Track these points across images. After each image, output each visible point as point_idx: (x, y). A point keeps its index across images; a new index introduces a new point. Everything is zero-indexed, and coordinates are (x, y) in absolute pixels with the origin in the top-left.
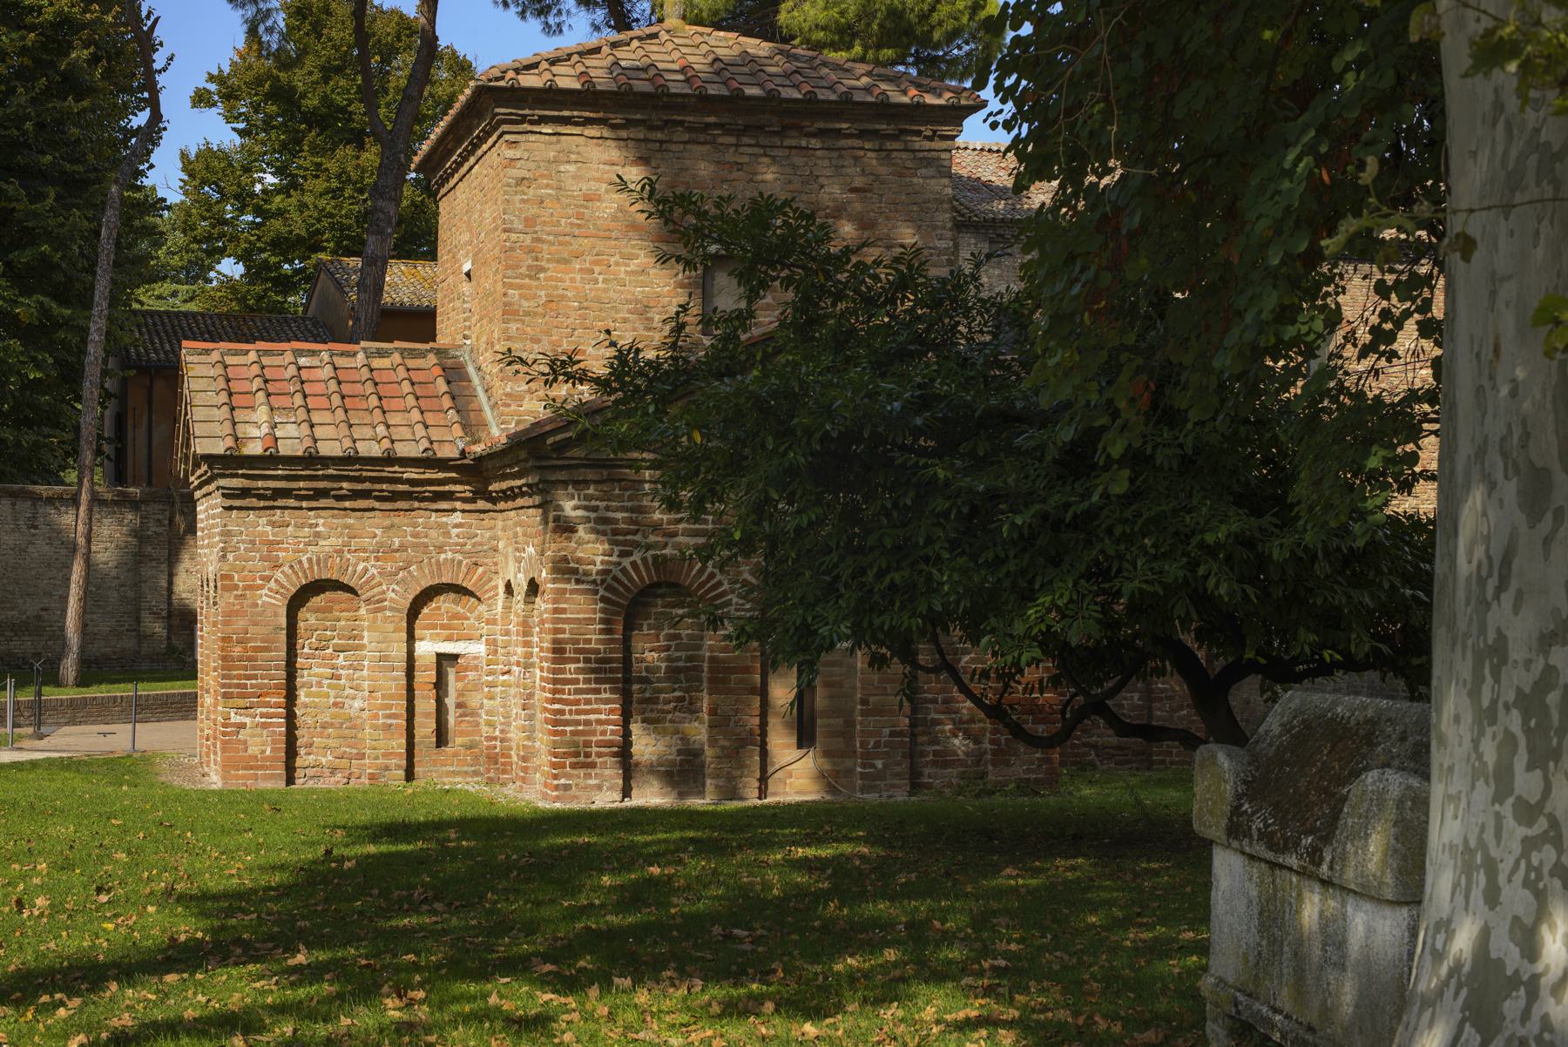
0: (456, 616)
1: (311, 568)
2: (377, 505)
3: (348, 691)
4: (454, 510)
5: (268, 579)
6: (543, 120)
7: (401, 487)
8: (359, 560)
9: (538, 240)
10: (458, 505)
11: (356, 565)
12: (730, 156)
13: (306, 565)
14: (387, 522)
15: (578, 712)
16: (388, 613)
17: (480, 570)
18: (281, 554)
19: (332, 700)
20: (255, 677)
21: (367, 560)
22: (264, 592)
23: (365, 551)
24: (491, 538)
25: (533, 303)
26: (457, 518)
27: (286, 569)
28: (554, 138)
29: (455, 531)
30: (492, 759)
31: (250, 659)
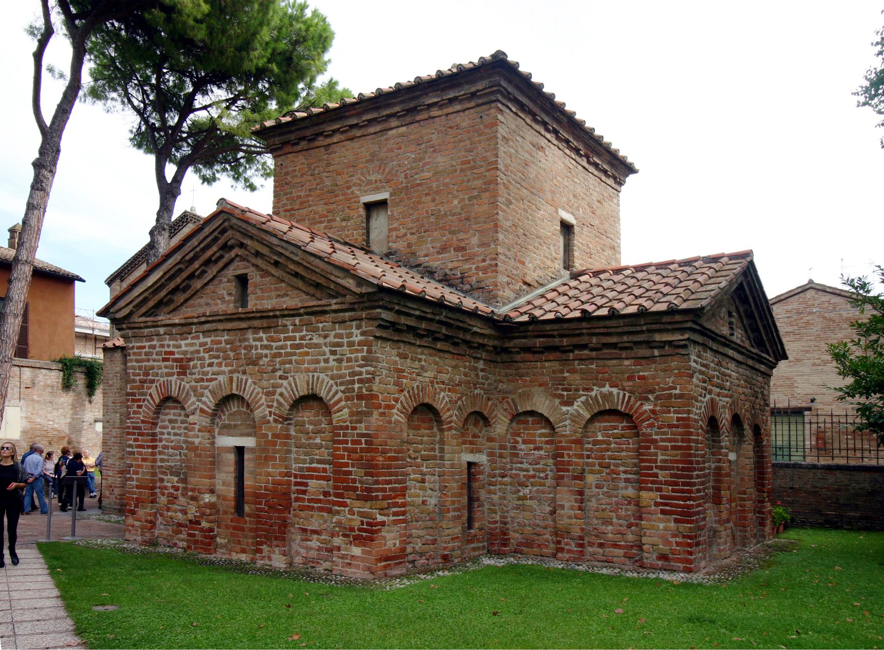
0: (474, 436)
1: (418, 394)
2: (451, 349)
3: (430, 492)
4: (479, 359)
5: (396, 400)
8: (441, 390)
10: (484, 355)
11: (439, 394)
13: (416, 391)
14: (454, 363)
16: (454, 432)
17: (490, 403)
18: (405, 381)
21: (444, 390)
22: (395, 411)
23: (443, 383)
24: (495, 381)
26: (481, 365)
27: (406, 392)
29: (481, 374)
30: (491, 536)
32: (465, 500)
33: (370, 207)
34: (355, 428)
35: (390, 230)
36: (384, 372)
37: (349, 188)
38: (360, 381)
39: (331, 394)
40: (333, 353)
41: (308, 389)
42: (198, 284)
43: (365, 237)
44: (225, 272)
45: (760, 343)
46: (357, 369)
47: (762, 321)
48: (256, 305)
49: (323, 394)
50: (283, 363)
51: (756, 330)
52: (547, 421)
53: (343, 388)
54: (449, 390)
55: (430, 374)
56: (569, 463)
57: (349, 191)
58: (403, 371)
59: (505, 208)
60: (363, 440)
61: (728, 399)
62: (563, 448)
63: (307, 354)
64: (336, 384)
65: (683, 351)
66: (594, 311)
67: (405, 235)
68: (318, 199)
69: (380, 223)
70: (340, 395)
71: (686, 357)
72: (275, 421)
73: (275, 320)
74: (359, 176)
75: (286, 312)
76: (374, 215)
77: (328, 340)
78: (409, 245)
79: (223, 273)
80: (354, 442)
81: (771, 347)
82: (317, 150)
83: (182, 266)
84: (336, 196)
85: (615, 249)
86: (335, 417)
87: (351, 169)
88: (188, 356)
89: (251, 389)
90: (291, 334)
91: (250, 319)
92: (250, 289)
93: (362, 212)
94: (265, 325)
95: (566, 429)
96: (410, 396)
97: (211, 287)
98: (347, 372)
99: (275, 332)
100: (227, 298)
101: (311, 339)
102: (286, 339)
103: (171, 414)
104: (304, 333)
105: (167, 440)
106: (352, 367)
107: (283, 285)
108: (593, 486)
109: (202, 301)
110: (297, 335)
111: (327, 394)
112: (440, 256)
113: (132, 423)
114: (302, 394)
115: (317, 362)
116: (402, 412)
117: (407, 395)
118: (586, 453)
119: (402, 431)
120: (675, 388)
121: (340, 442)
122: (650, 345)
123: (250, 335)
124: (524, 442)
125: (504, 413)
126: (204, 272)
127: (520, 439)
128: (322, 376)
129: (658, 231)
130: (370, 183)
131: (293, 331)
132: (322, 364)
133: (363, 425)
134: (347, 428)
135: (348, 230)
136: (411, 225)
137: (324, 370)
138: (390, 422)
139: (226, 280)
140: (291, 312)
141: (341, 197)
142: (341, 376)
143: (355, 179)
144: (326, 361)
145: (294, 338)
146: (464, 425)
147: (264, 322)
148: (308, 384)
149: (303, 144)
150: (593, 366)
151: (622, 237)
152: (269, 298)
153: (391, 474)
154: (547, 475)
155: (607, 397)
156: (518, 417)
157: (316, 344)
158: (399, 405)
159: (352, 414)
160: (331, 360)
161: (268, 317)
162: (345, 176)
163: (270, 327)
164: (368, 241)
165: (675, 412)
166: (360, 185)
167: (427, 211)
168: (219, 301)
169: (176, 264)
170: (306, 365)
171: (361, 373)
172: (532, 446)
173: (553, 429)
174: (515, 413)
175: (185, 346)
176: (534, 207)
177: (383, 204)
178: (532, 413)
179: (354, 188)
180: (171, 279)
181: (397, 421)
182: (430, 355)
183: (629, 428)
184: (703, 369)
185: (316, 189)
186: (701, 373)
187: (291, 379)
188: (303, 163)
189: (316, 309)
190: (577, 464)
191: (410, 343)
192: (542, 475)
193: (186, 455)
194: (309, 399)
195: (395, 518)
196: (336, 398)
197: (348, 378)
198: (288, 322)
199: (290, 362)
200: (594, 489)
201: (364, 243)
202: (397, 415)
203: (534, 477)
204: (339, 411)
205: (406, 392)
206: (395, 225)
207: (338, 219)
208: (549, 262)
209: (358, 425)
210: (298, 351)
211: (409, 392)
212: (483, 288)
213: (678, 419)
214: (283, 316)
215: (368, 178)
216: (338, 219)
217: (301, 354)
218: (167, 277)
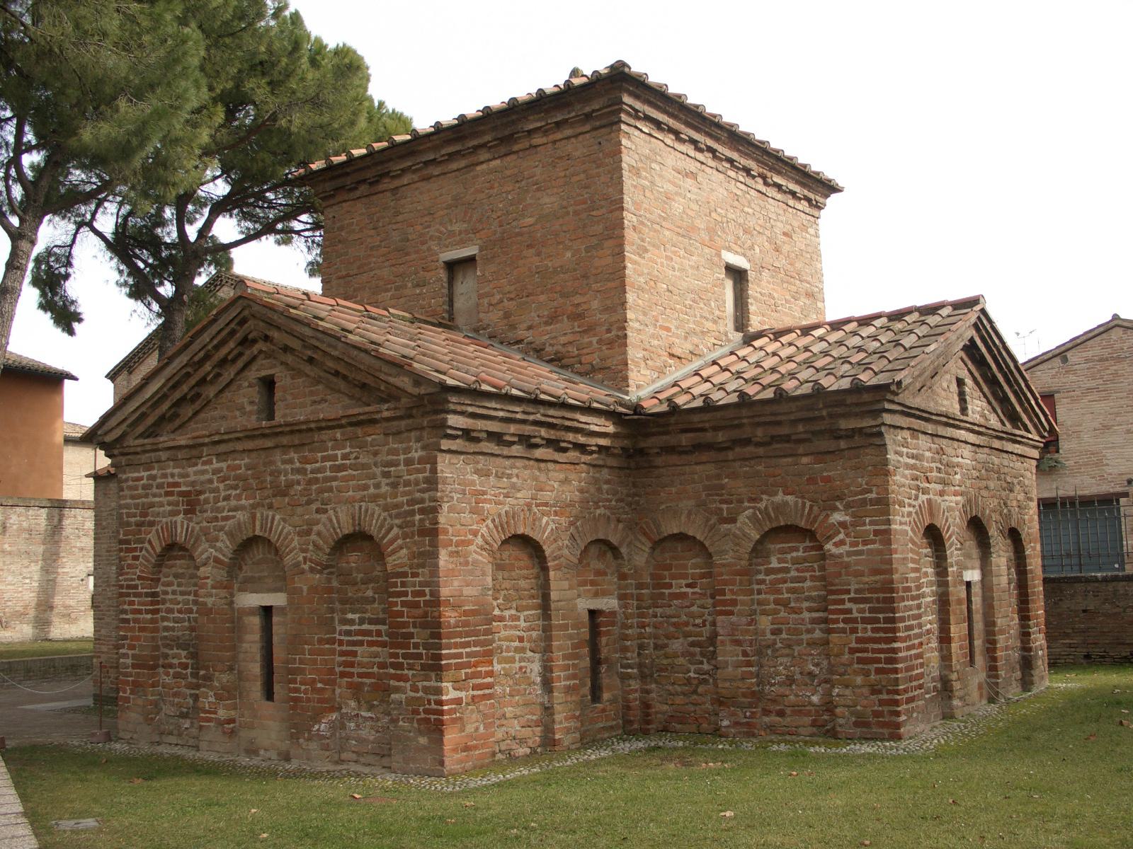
5: (475, 533)
6: (648, 118)
7: (582, 439)
9: (642, 223)
11: (540, 520)
12: (732, 186)
13: (504, 519)
14: (562, 476)
15: (909, 648)
19: (517, 665)
20: (467, 645)
21: (548, 514)
22: (473, 548)
23: (546, 504)
25: (642, 280)
27: (489, 522)
28: (648, 138)
29: (605, 487)
31: (466, 624)
32: (586, 662)
33: (453, 267)
34: (415, 575)
35: (481, 297)
36: (456, 496)
37: (423, 243)
38: (422, 511)
39: (383, 531)
40: (386, 475)
41: (354, 525)
42: (211, 391)
43: (446, 307)
44: (246, 373)
45: (1014, 418)
46: (418, 495)
47: (1011, 386)
48: (285, 416)
49: (373, 531)
50: (321, 491)
51: (1004, 400)
52: (702, 544)
53: (397, 521)
54: (556, 513)
55: (524, 495)
56: (734, 603)
57: (424, 247)
58: (484, 493)
59: (636, 258)
60: (427, 590)
61: (959, 498)
62: (726, 583)
63: (353, 478)
64: (390, 516)
65: (877, 441)
66: (758, 393)
67: (501, 301)
68: (381, 259)
69: (466, 287)
70: (395, 530)
71: (882, 449)
72: (312, 570)
73: (310, 434)
74: (438, 226)
75: (323, 424)
76: (460, 277)
77: (379, 458)
78: (507, 315)
79: (241, 376)
80: (416, 594)
81: (1031, 420)
82: (381, 195)
83: (189, 370)
84: (407, 254)
85: (814, 296)
86: (391, 561)
87: (426, 219)
88: (198, 488)
89: (281, 526)
90: (331, 452)
91: (277, 434)
92: (278, 394)
93: (443, 275)
94: (297, 442)
95: (728, 556)
96: (496, 527)
97: (227, 394)
98: (405, 499)
99: (310, 451)
100: (248, 408)
101: (356, 458)
102: (324, 459)
103: (180, 565)
104: (348, 450)
105: (172, 601)
106: (409, 493)
107: (320, 387)
108: (768, 631)
109: (216, 413)
110: (339, 453)
111: (379, 532)
112: (549, 328)
113: (126, 580)
114: (347, 532)
115: (366, 487)
116: (485, 549)
117: (491, 526)
118: (756, 587)
119: (484, 574)
120: (871, 492)
121: (400, 594)
122: (836, 435)
123: (278, 456)
124: (673, 577)
125: (644, 539)
126: (218, 375)
127: (666, 573)
128: (371, 505)
129: (864, 267)
130: (451, 234)
131: (333, 449)
132: (372, 490)
133: (426, 571)
134: (404, 575)
135: (424, 299)
136: (508, 288)
137: (374, 498)
138: (467, 563)
139: (246, 384)
140: (330, 424)
141: (414, 256)
142: (397, 506)
143: (432, 231)
144: (377, 486)
145: (334, 458)
146: (580, 561)
147: (296, 439)
148: (353, 518)
149: (363, 189)
150: (760, 468)
151: (825, 278)
152: (303, 406)
153: (468, 634)
154: (704, 621)
155: (779, 508)
156: (660, 543)
157: (363, 465)
158: (479, 541)
159: (413, 556)
160: (383, 484)
161: (300, 431)
162: (419, 228)
163: (304, 445)
164: (451, 312)
165: (871, 523)
166: (440, 239)
167: (530, 269)
168: (238, 413)
169: (183, 367)
170: (351, 493)
171: (422, 501)
172: (684, 582)
173: (710, 556)
174: (657, 538)
175: (204, 471)
176: (682, 252)
177: (471, 260)
178: (681, 537)
179: (431, 243)
180: (174, 387)
181: (475, 562)
182: (525, 467)
183: (812, 548)
184: (912, 461)
185: (379, 246)
186: (908, 466)
187: (331, 512)
188: (363, 214)
189: (362, 417)
190: (743, 603)
191: (493, 455)
192: (698, 621)
193: (196, 620)
194: (357, 539)
195: (476, 693)
196: (390, 536)
197: (406, 508)
198: (325, 435)
199: (330, 489)
200: (769, 636)
201: (446, 315)
202: (475, 552)
203: (687, 624)
204: (394, 552)
205: (489, 522)
206: (487, 289)
207: (410, 285)
208: (709, 325)
209: (420, 571)
210: (340, 474)
211: (493, 521)
212: (609, 368)
213: (876, 533)
214: (320, 429)
215: (449, 228)
216: (410, 285)
217: (344, 479)
218: (170, 384)
